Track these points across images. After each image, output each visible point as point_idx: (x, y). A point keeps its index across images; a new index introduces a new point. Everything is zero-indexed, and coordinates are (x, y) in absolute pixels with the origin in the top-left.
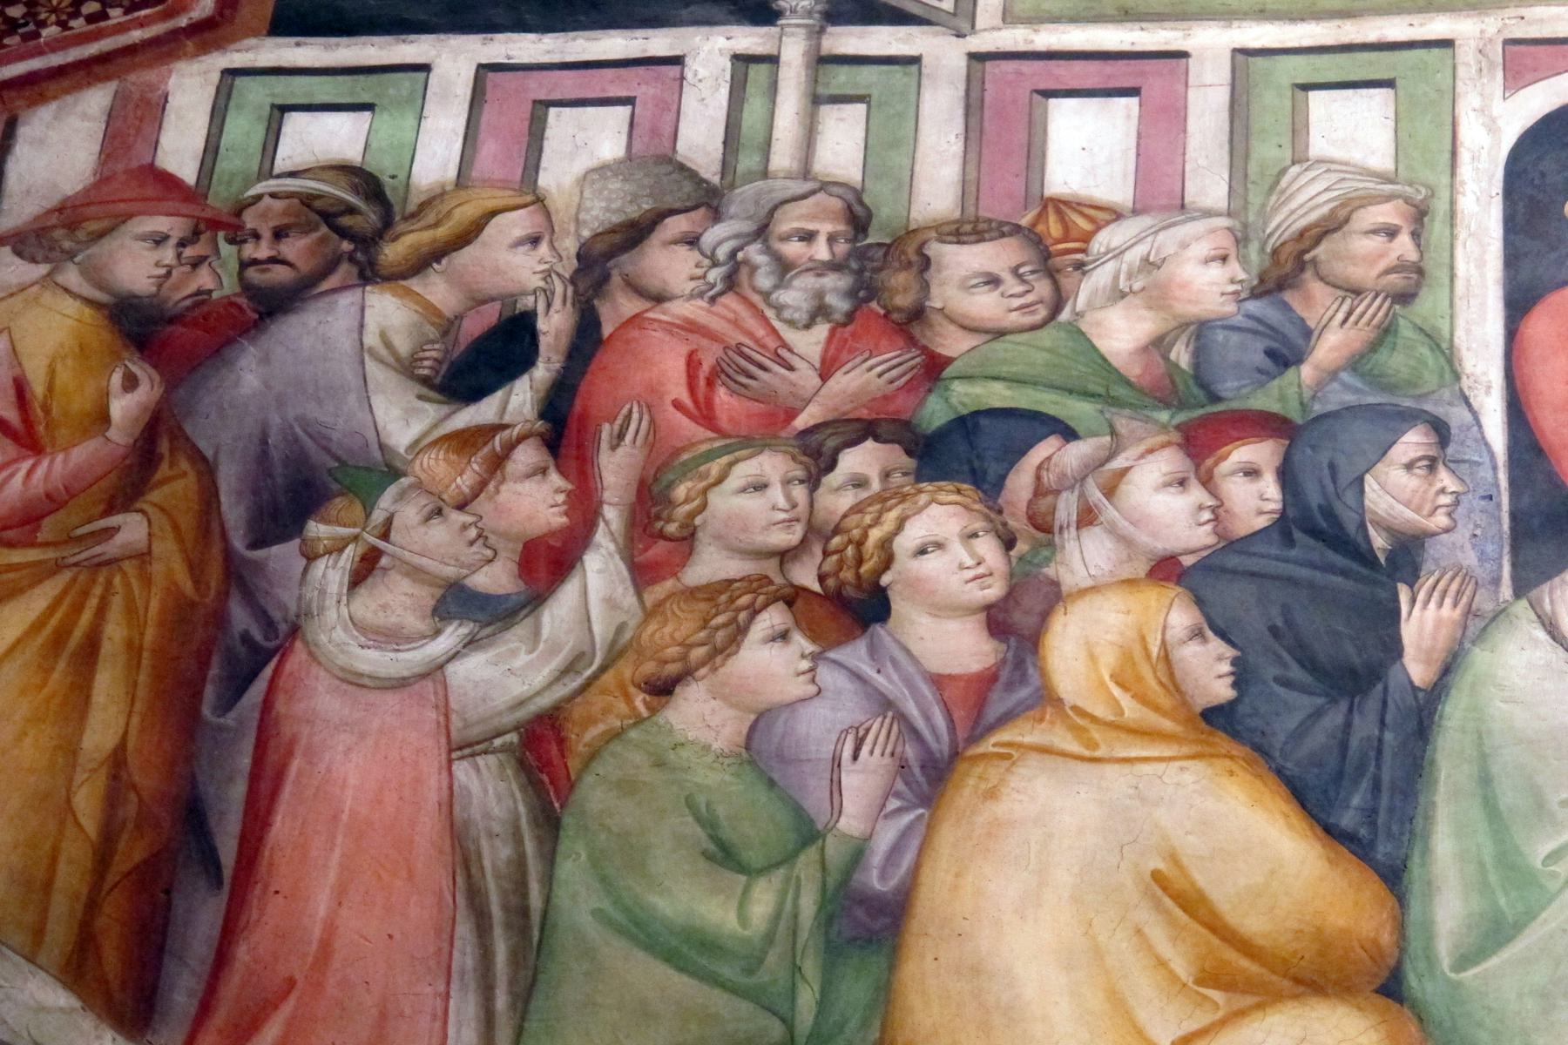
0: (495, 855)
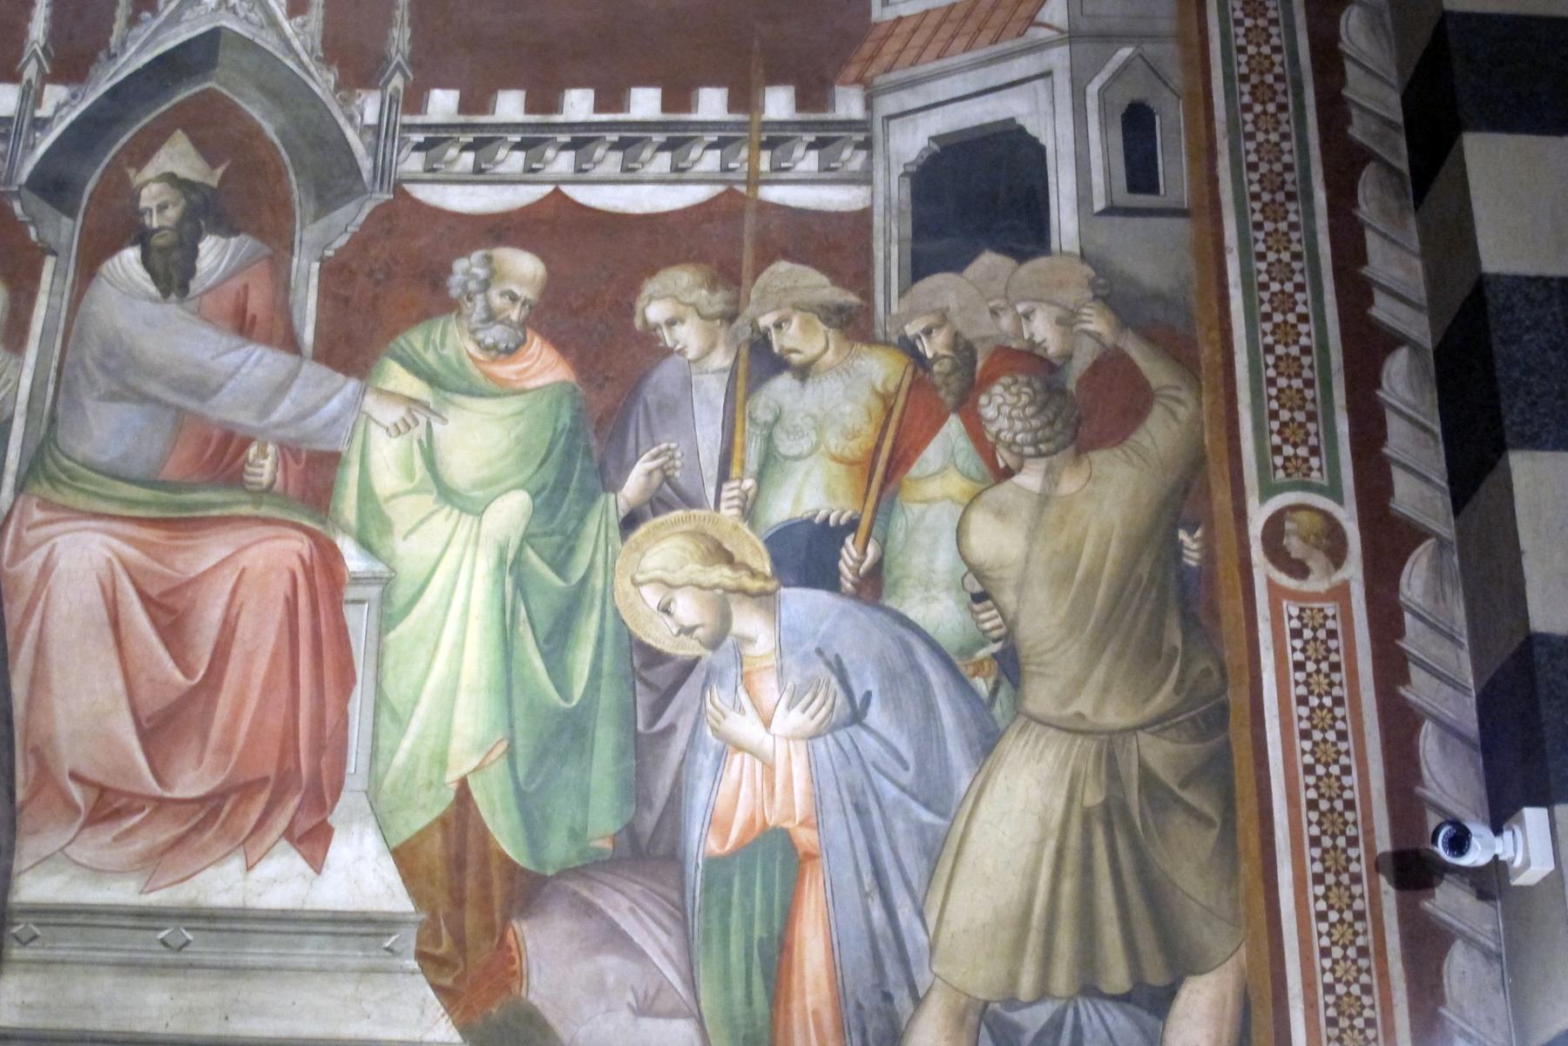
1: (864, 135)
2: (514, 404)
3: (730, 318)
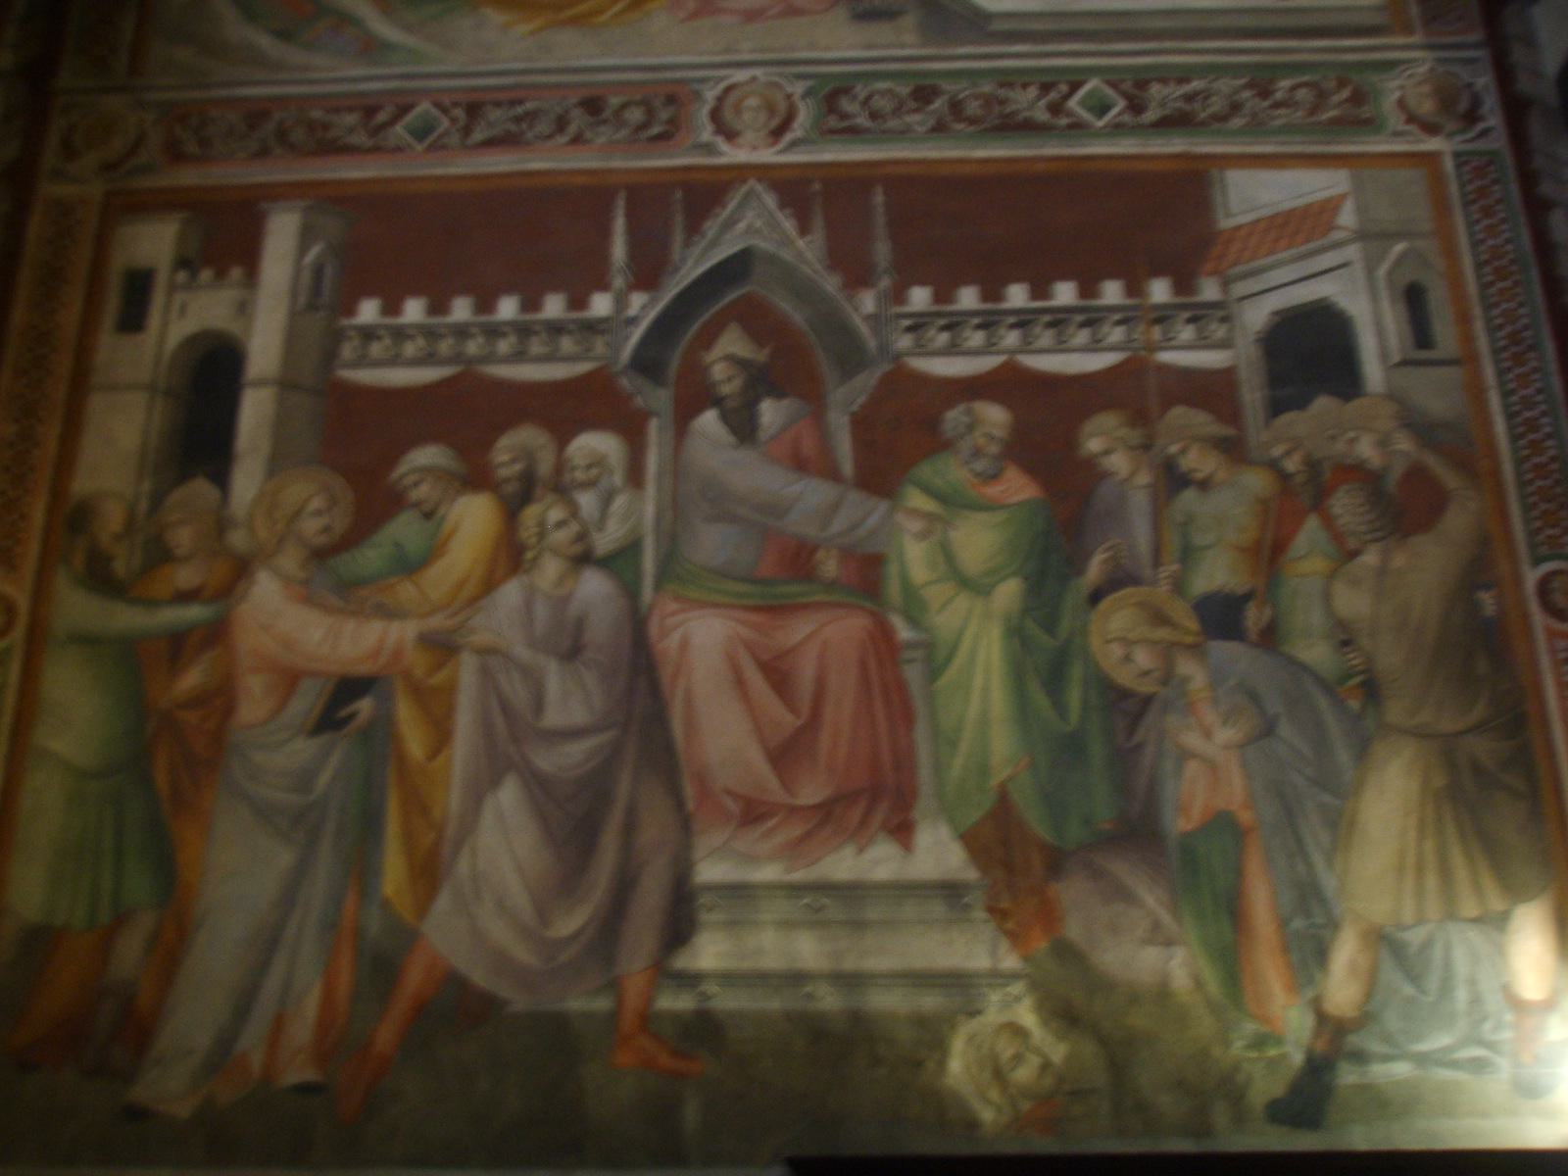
1: (1223, 311)
2: (999, 517)
3: (1146, 447)
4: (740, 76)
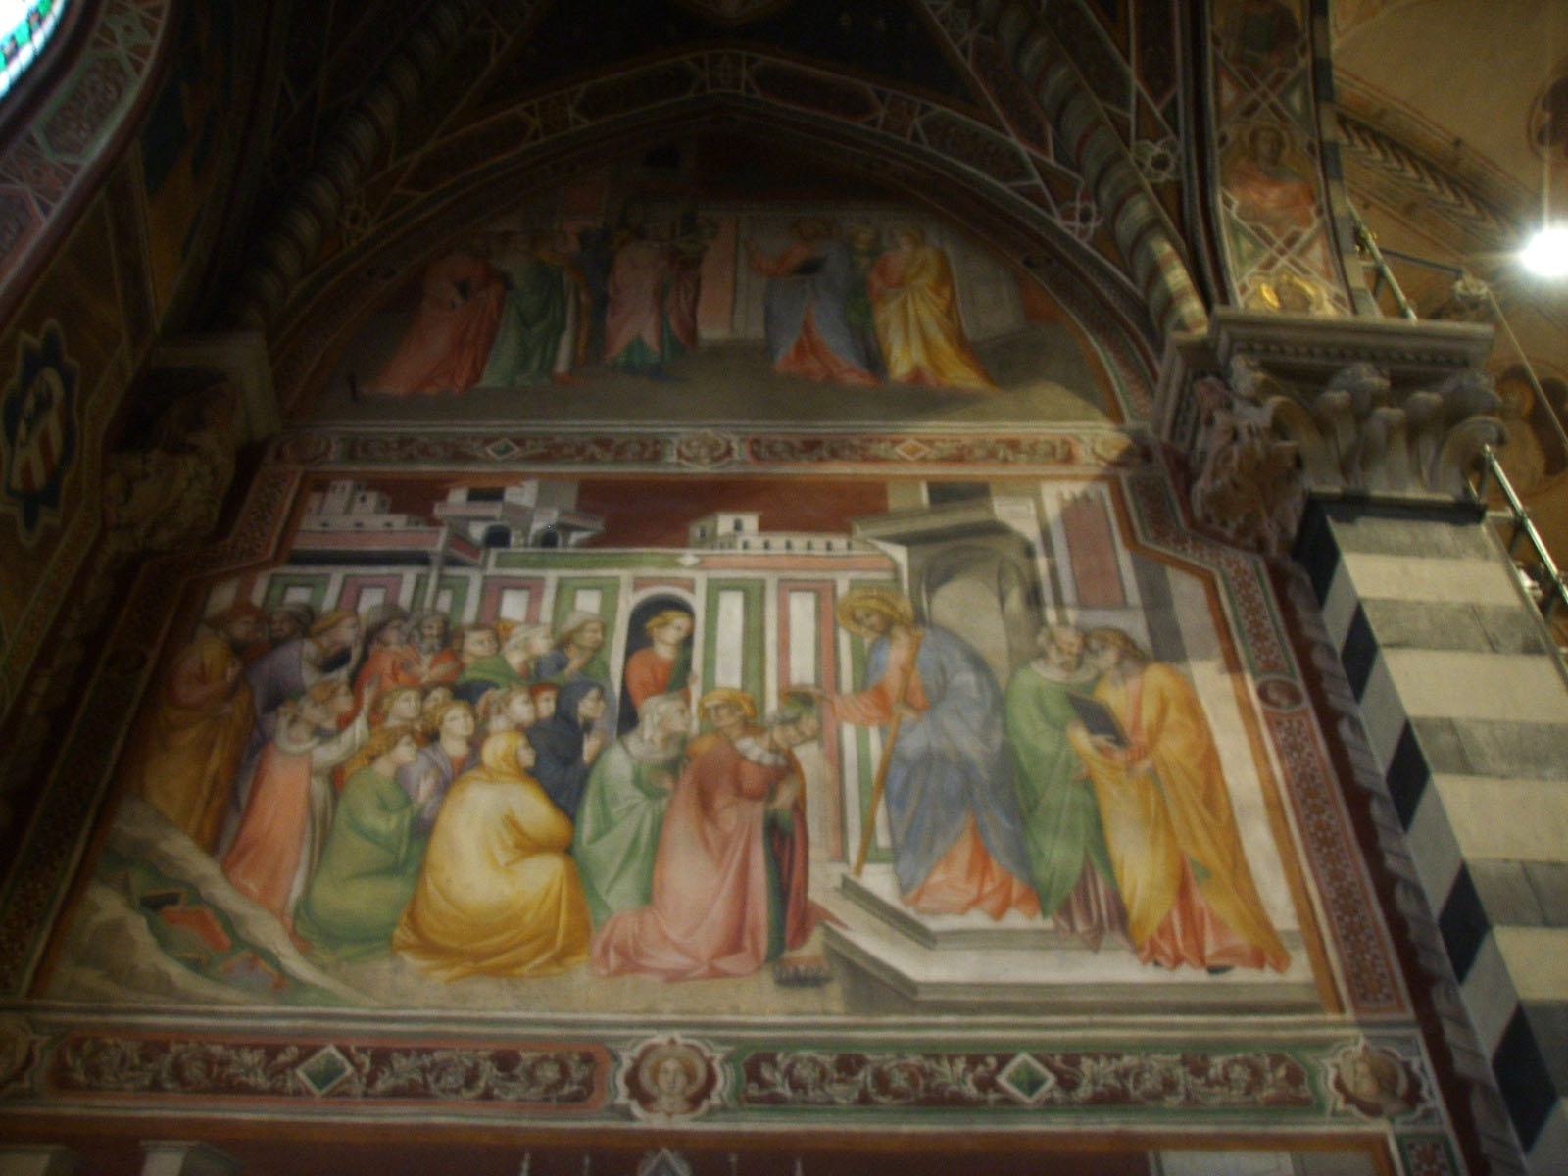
0: (319, 806)
4: (660, 1038)
